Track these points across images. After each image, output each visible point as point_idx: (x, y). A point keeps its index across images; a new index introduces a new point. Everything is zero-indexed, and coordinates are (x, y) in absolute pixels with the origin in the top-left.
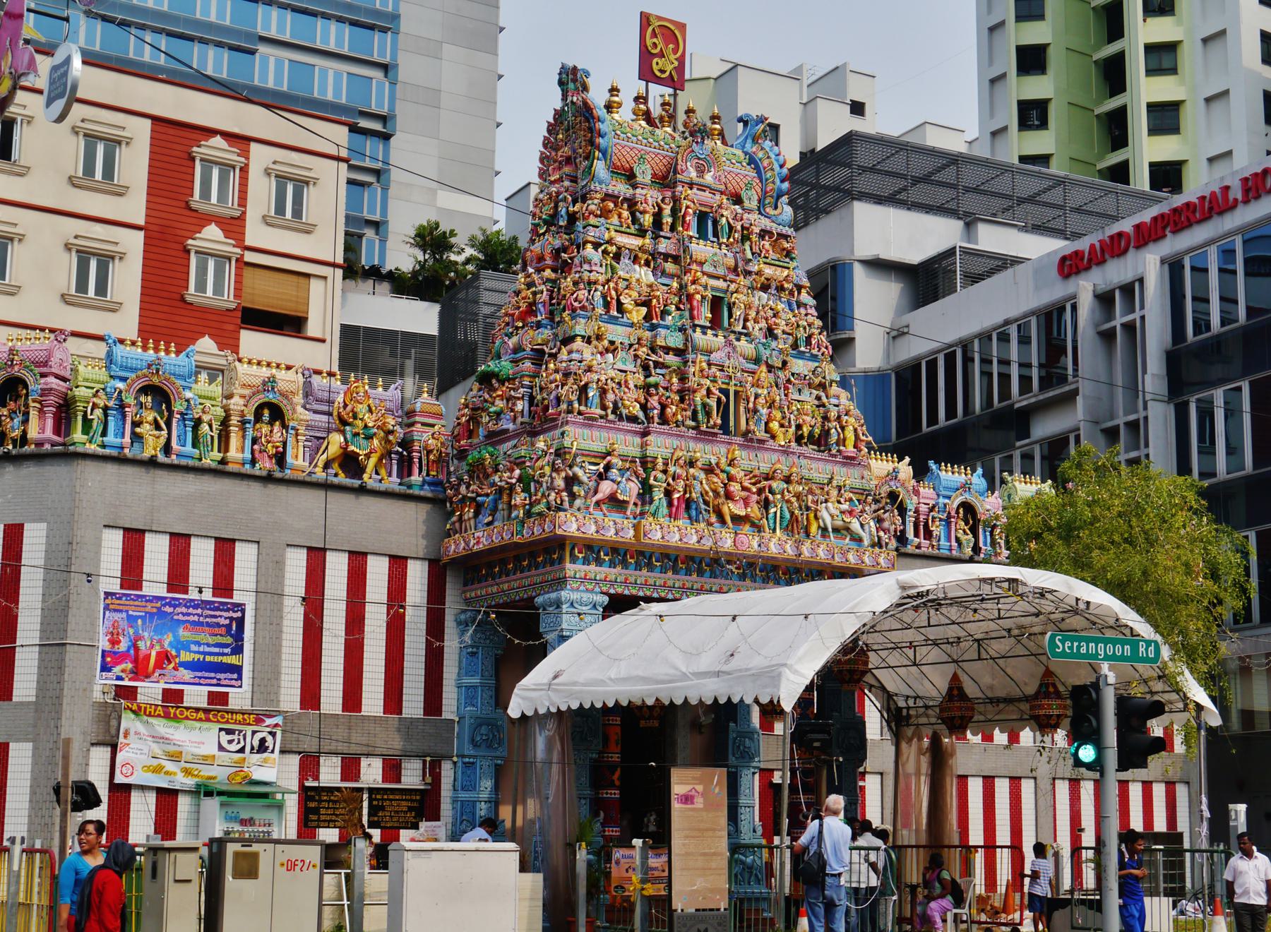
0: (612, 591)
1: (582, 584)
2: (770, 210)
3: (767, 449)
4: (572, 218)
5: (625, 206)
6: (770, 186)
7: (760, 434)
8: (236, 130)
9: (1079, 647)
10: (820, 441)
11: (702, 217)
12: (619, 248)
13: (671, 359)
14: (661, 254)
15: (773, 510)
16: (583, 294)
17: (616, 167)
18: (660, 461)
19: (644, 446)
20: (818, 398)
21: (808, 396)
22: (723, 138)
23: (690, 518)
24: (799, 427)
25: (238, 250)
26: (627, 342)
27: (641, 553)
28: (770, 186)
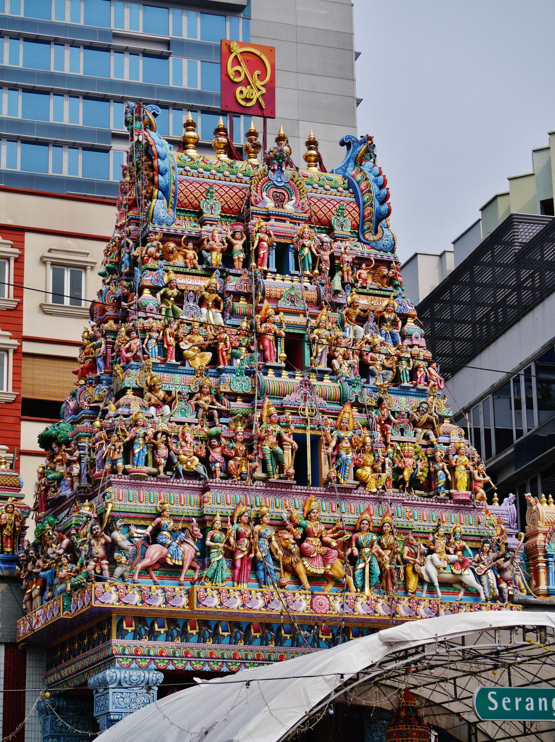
0: (171, 667)
1: (131, 661)
2: (370, 237)
3: (355, 498)
4: (134, 262)
5: (191, 245)
6: (368, 210)
7: (350, 481)
8: (10, 222)
9: (523, 704)
10: (427, 485)
11: (281, 251)
12: (182, 291)
13: (239, 406)
14: (230, 293)
15: (361, 566)
16: (136, 343)
17: (185, 205)
18: (218, 518)
19: (201, 503)
20: (426, 437)
21: (413, 438)
22: (321, 163)
23: (258, 580)
24: (399, 471)
25: (15, 342)
26: (186, 390)
27: (204, 623)
28: (368, 210)
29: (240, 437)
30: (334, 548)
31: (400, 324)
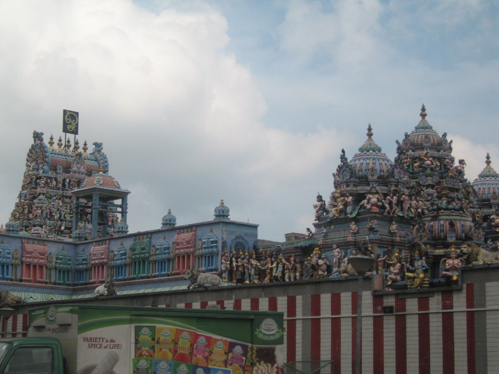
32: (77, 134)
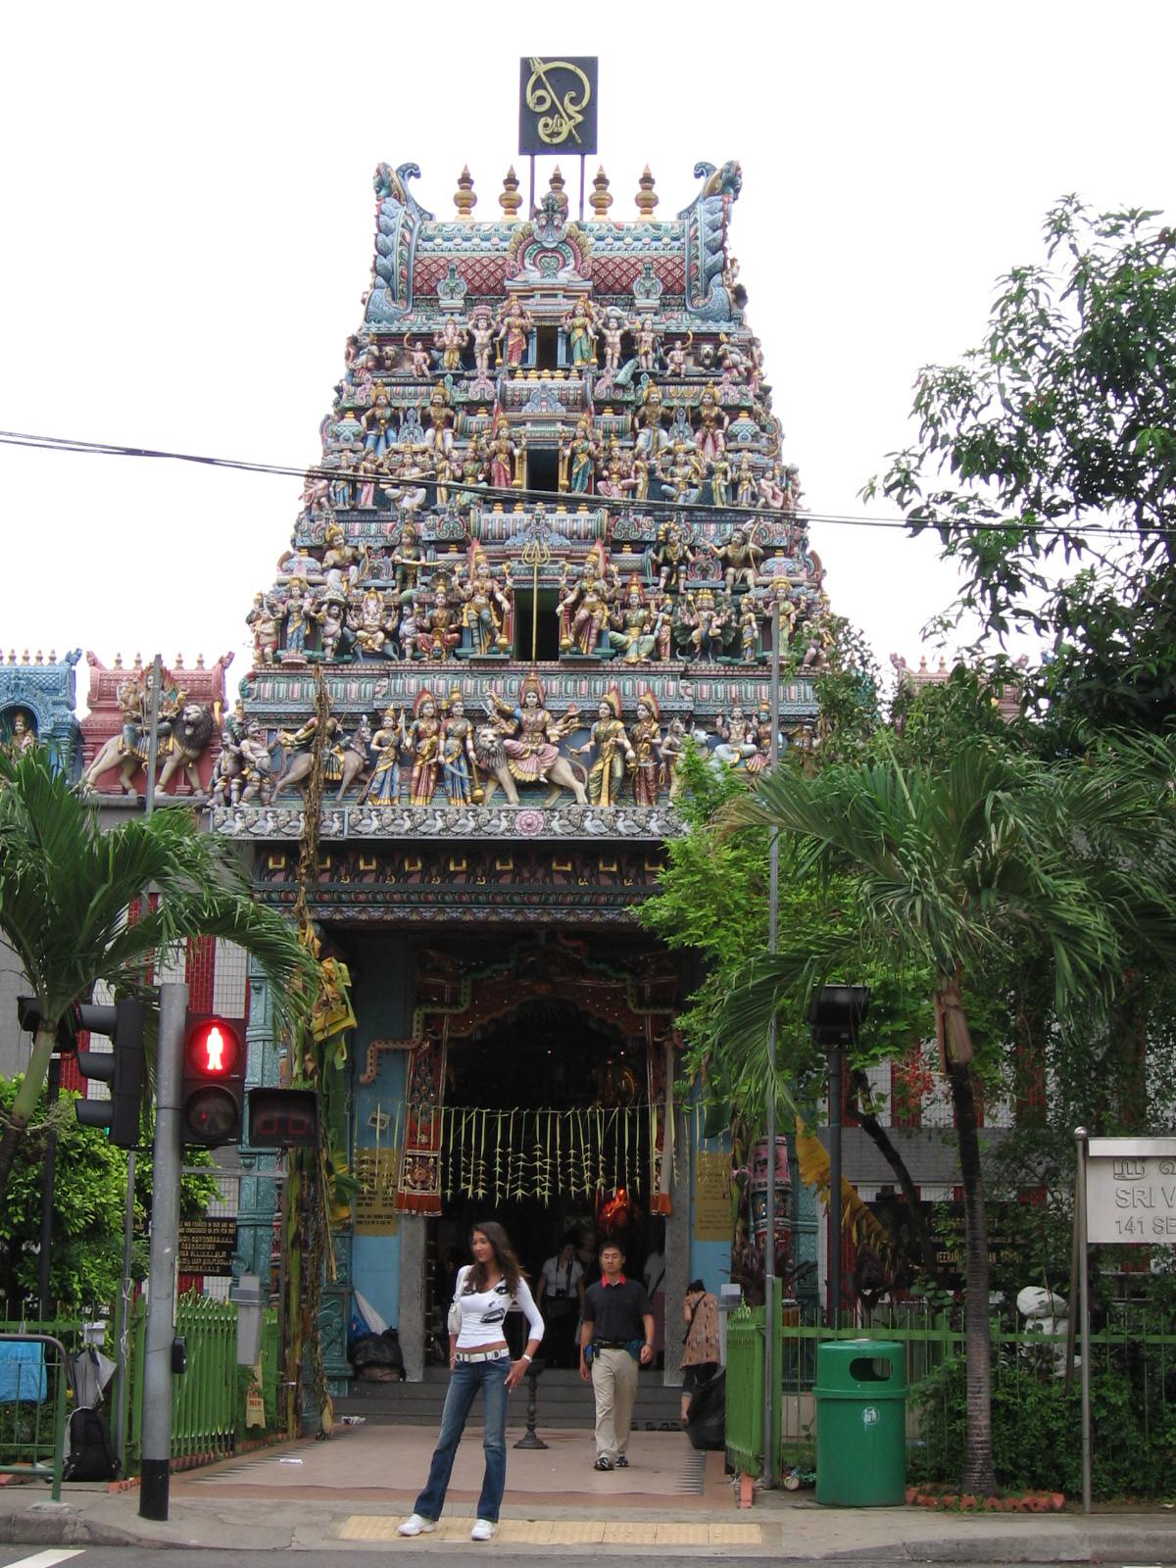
5: (419, 345)
29: (440, 600)
30: (554, 744)
31: (727, 420)
32: (593, 150)
